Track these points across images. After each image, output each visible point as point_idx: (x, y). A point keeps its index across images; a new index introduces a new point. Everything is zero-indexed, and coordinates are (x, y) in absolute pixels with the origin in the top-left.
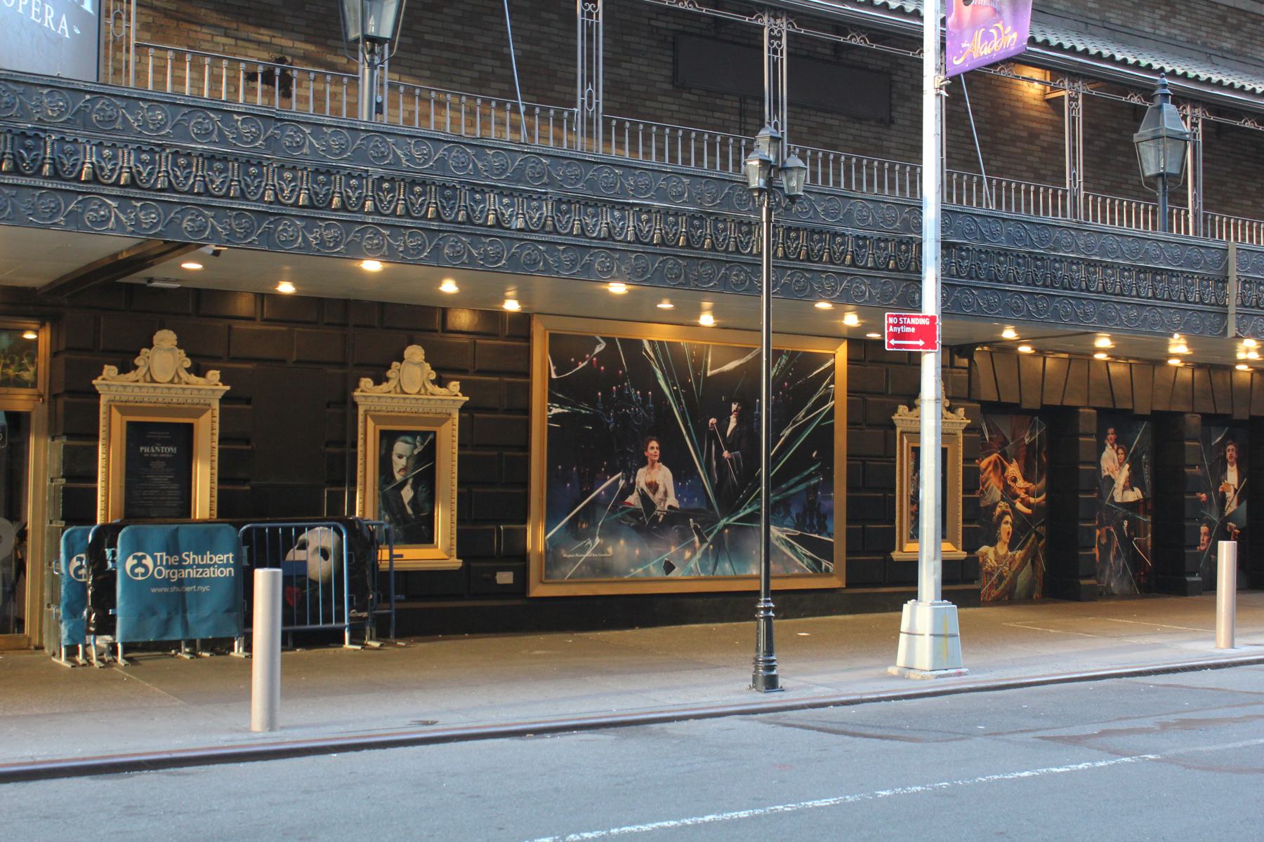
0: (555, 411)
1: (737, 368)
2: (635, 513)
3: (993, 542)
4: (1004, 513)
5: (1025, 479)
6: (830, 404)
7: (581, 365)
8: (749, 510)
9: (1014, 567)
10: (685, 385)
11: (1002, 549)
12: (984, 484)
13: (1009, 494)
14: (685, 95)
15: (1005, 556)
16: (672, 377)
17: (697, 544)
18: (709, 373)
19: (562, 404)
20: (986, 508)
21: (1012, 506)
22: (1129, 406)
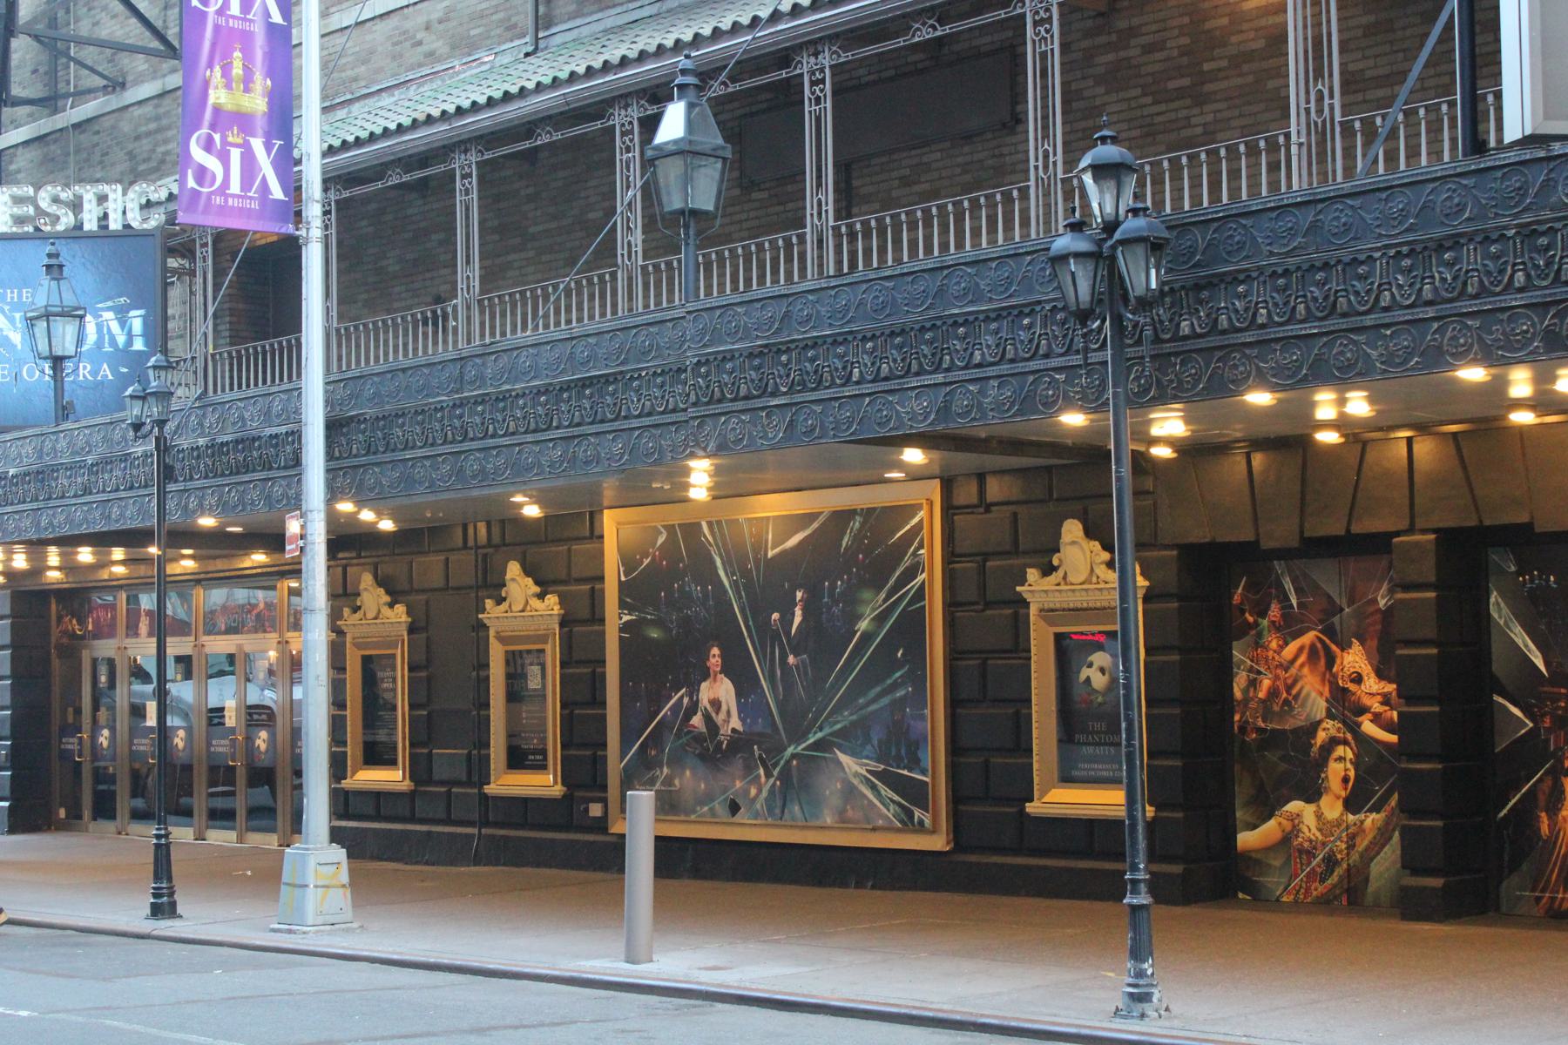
0: (626, 618)
1: (801, 543)
2: (698, 738)
3: (1312, 794)
4: (1333, 742)
5: (1381, 675)
6: (920, 578)
7: (646, 562)
8: (820, 735)
9: (1362, 844)
10: (745, 573)
11: (1332, 808)
12: (1289, 688)
13: (1344, 704)
14: (755, 195)
15: (1338, 823)
16: (731, 565)
17: (763, 779)
18: (770, 554)
19: (631, 610)
20: (1295, 731)
21: (1354, 729)
22: (1523, 518)
